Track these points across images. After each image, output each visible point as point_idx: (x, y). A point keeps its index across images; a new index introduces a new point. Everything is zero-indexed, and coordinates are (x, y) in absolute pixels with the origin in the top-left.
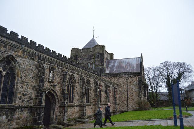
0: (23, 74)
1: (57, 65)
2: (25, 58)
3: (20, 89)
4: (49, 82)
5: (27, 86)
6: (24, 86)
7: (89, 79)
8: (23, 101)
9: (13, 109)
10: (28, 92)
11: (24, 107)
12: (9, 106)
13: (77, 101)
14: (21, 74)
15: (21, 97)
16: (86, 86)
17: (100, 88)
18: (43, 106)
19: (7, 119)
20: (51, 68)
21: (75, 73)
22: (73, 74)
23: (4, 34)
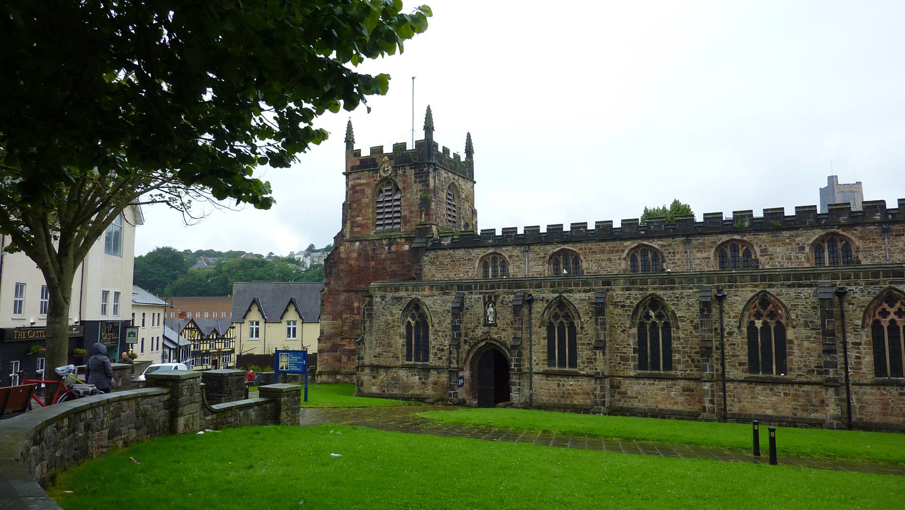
0: (436, 320)
1: (505, 288)
2: (435, 295)
3: (433, 343)
4: (486, 324)
5: (443, 337)
6: (439, 337)
7: (659, 293)
8: (440, 359)
9: (426, 370)
10: (445, 346)
11: (442, 368)
12: (421, 365)
13: (589, 363)
14: (432, 321)
15: (436, 353)
16: (648, 317)
17: (772, 315)
18: (454, 368)
19: (420, 382)
20: (487, 300)
21: (570, 291)
22: (565, 295)
23: (490, 241)
